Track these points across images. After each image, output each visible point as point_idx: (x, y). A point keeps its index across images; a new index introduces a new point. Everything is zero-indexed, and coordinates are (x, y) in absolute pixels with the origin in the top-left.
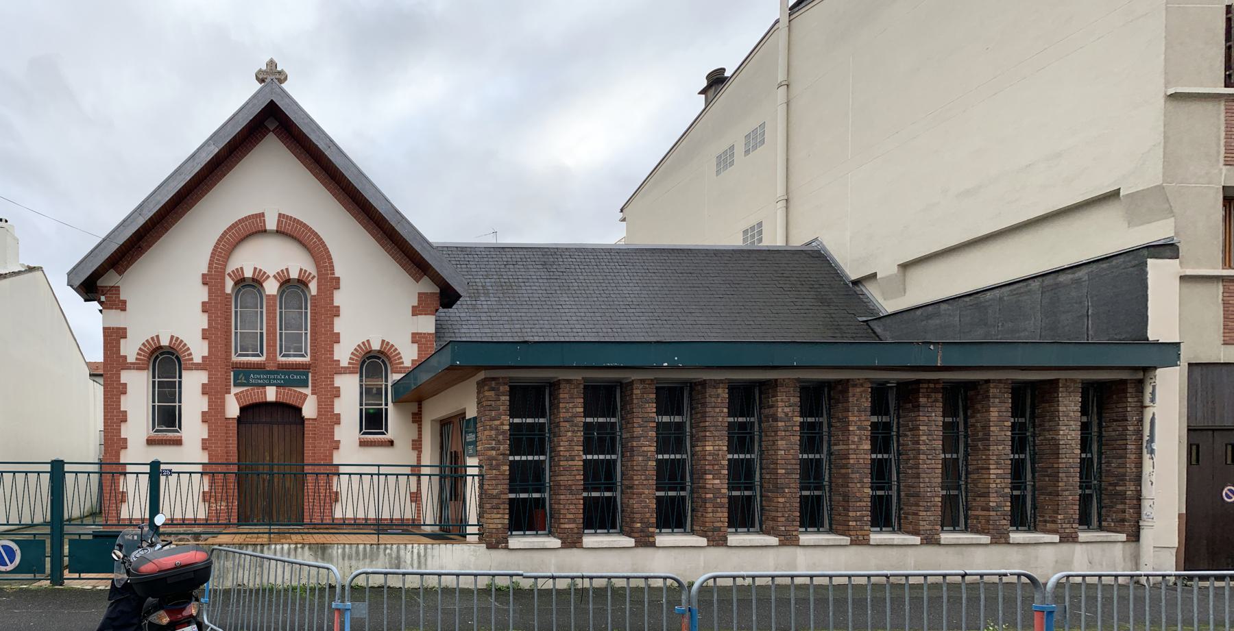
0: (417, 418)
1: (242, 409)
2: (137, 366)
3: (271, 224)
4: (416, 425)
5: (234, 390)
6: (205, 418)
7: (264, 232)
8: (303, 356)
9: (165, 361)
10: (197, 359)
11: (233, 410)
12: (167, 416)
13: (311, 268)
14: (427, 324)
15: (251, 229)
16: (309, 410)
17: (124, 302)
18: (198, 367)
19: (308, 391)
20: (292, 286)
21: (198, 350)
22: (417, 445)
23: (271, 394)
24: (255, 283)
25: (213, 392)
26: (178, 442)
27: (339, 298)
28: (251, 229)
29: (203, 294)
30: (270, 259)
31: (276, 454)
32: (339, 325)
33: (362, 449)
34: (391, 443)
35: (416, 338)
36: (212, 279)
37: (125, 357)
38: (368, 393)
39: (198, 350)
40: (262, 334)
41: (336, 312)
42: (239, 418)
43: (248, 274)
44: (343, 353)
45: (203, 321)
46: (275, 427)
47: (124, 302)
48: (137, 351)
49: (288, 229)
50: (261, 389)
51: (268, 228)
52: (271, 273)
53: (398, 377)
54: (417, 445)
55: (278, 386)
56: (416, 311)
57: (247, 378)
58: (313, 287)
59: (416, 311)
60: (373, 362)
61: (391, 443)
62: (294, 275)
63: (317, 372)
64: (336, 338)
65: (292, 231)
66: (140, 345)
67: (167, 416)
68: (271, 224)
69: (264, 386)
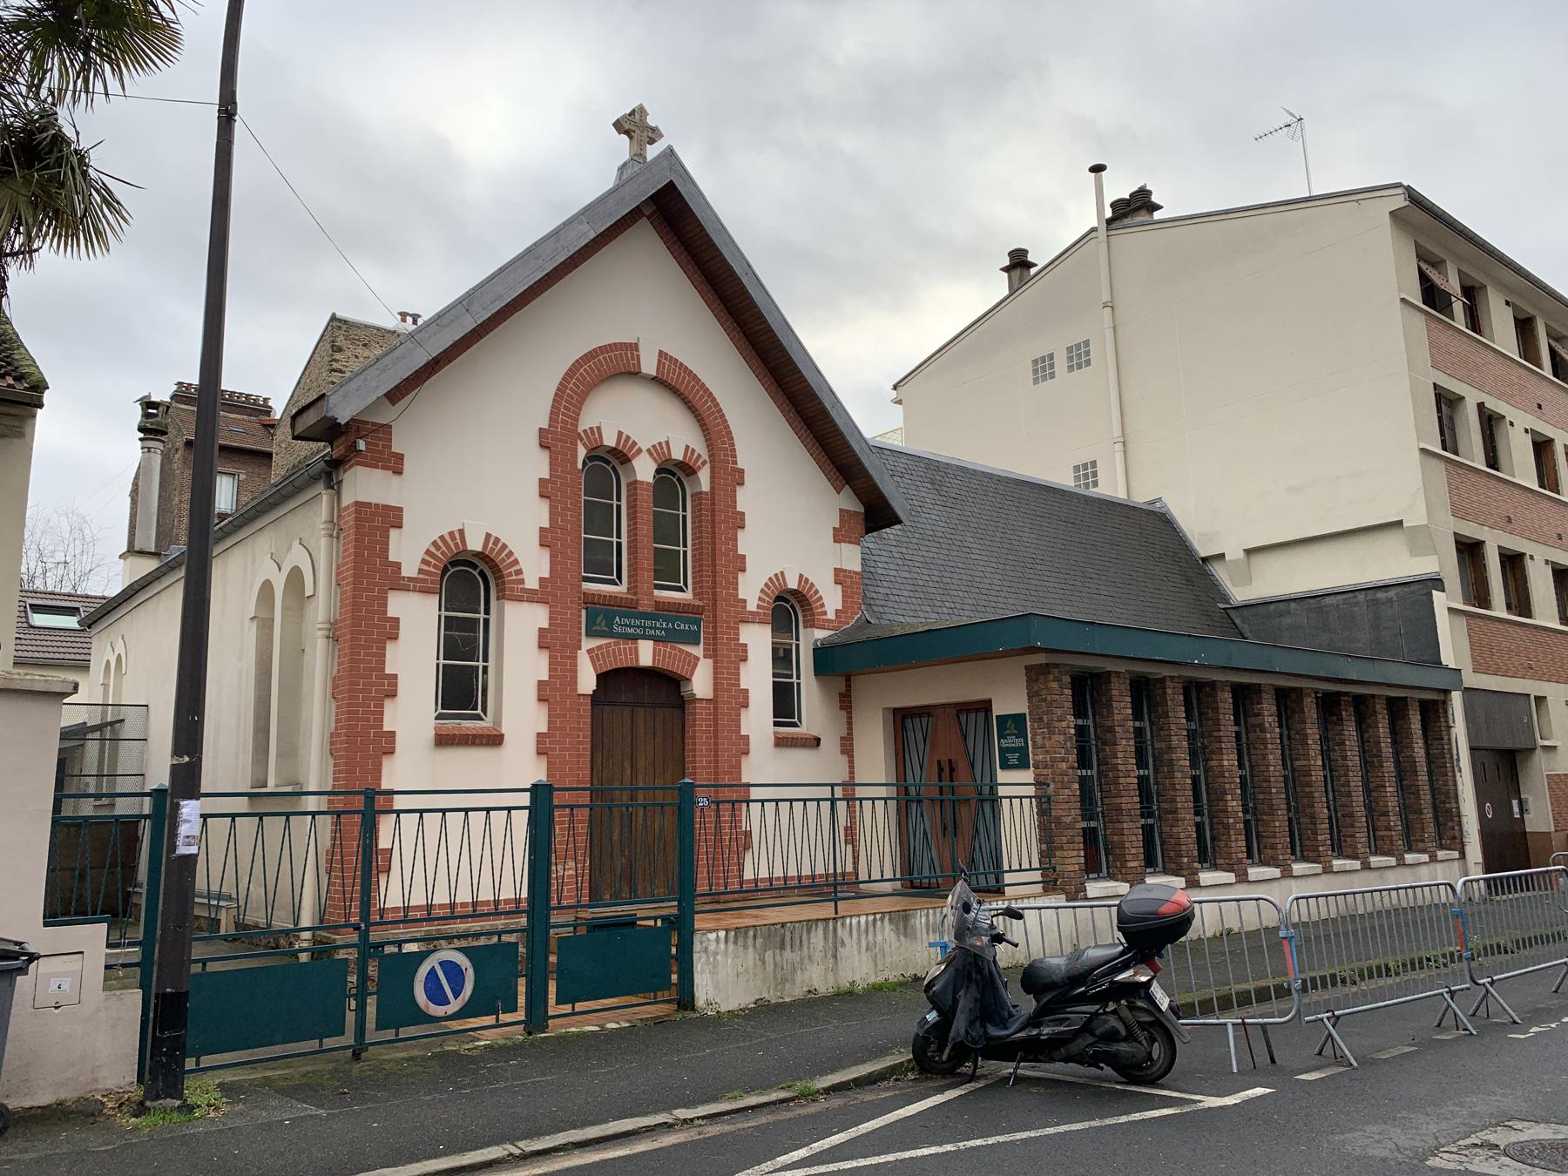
0: (845, 702)
1: (602, 678)
2: (417, 586)
3: (649, 366)
4: (844, 713)
5: (588, 644)
6: (545, 693)
7: (634, 374)
8: (680, 589)
9: (469, 579)
10: (532, 583)
11: (587, 682)
12: (461, 690)
13: (700, 448)
14: (851, 558)
15: (613, 366)
16: (701, 684)
17: (400, 457)
18: (531, 597)
19: (698, 651)
20: (673, 473)
21: (534, 565)
22: (847, 746)
23: (646, 653)
24: (621, 456)
25: (553, 642)
26: (494, 740)
27: (745, 500)
28: (613, 366)
29: (540, 465)
30: (642, 423)
31: (641, 764)
32: (746, 543)
33: (778, 750)
34: (816, 742)
35: (841, 576)
36: (554, 439)
37: (398, 565)
38: (782, 658)
39: (534, 565)
40: (619, 544)
41: (739, 522)
42: (594, 697)
43: (610, 441)
44: (751, 589)
45: (540, 514)
46: (640, 711)
47: (400, 457)
48: (421, 555)
49: (672, 379)
50: (630, 645)
51: (645, 370)
52: (644, 445)
53: (820, 634)
54: (847, 746)
55: (656, 640)
56: (839, 536)
57: (610, 624)
58: (704, 476)
59: (839, 536)
60: (789, 607)
61: (816, 742)
62: (677, 454)
63: (707, 621)
64: (740, 564)
65: (676, 384)
66: (427, 544)
67: (461, 690)
68: (649, 366)
69: (635, 638)
